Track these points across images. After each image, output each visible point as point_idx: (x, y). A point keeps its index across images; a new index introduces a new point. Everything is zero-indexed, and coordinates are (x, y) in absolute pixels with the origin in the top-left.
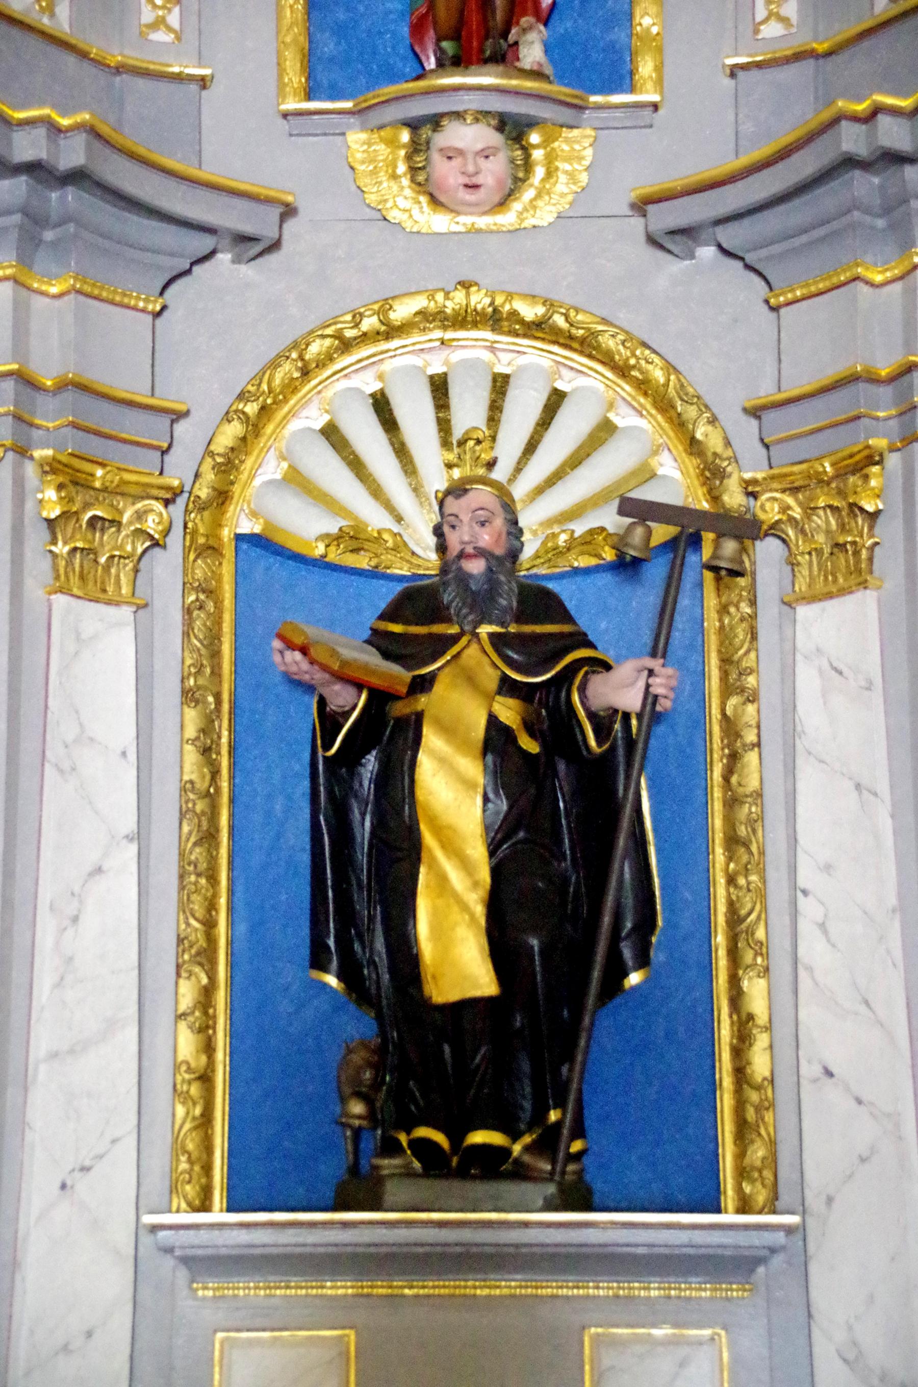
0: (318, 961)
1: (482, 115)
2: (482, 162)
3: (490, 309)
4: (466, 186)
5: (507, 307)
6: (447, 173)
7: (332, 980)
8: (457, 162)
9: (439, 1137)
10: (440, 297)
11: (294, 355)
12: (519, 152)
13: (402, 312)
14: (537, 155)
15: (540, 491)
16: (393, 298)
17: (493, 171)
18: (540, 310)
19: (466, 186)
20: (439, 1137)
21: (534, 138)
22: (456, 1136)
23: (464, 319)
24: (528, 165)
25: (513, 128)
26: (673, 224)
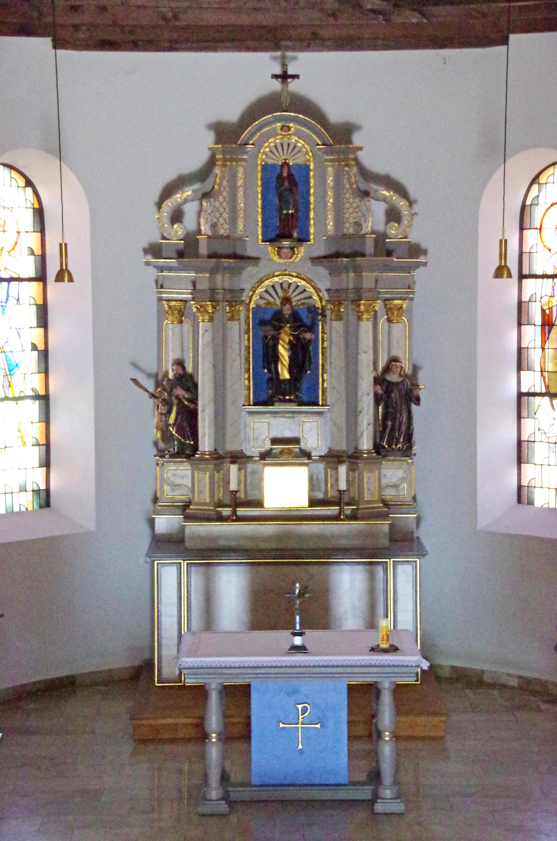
0: (264, 368)
1: (287, 247)
6: (283, 255)
7: (266, 371)
9: (281, 397)
13: (276, 274)
14: (296, 252)
15: (295, 296)
17: (290, 254)
20: (281, 397)
21: (295, 249)
22: (284, 396)
23: (286, 275)
24: (294, 253)
26: (316, 260)
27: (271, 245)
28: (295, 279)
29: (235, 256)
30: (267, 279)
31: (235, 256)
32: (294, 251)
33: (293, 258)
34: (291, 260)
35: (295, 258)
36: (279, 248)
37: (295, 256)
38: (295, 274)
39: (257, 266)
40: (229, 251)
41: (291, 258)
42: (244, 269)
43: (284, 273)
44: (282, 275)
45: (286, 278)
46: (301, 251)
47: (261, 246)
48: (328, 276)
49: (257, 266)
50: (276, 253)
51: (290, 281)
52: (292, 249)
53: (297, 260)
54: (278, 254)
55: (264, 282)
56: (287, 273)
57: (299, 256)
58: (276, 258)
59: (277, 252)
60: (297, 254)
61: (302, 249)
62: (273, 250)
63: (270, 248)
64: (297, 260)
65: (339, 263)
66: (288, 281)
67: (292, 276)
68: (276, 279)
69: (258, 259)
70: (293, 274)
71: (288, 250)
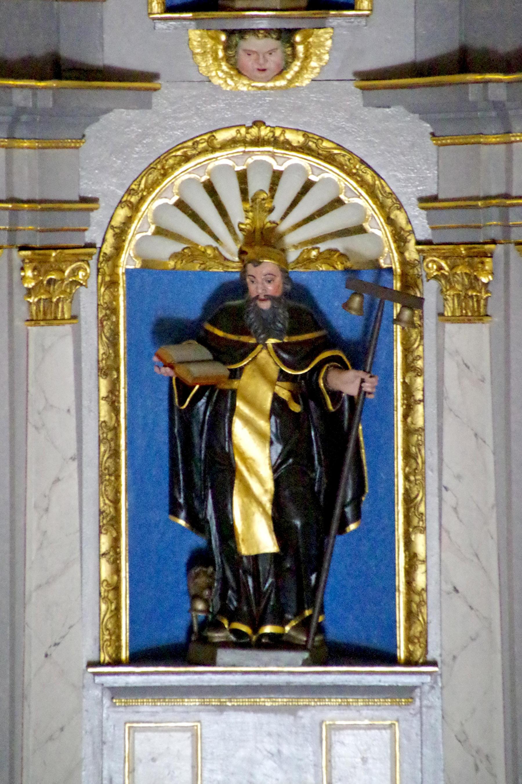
1: (268, 32)
2: (268, 56)
3: (272, 139)
4: (259, 70)
5: (282, 138)
6: (248, 62)
8: (253, 57)
10: (243, 130)
11: (159, 167)
12: (290, 49)
13: (222, 136)
14: (300, 49)
16: (215, 131)
18: (301, 139)
19: (259, 70)
21: (298, 38)
23: (258, 142)
24: (294, 56)
25: (286, 35)
27: (199, 24)
28: (296, 159)
29: (56, 68)
30: (187, 158)
31: (56, 68)
32: (293, 46)
33: (289, 76)
34: (281, 83)
35: (298, 74)
36: (230, 33)
37: (296, 66)
38: (296, 139)
39: (147, 105)
40: (38, 47)
41: (281, 73)
42: (95, 116)
43: (254, 131)
44: (244, 142)
45: (261, 155)
46: (321, 45)
47: (160, 25)
48: (430, 143)
49: (147, 105)
50: (221, 54)
51: (276, 167)
52: (286, 35)
53: (305, 81)
54: (227, 59)
55: (173, 168)
56: (264, 132)
57: (314, 64)
58: (220, 76)
59: (227, 47)
60: (307, 57)
61: (324, 38)
62: (210, 43)
63: (195, 35)
64: (305, 81)
65: (473, 93)
66: (271, 165)
67: (287, 145)
68: (222, 159)
69: (152, 77)
70: (290, 136)
71: (271, 43)
